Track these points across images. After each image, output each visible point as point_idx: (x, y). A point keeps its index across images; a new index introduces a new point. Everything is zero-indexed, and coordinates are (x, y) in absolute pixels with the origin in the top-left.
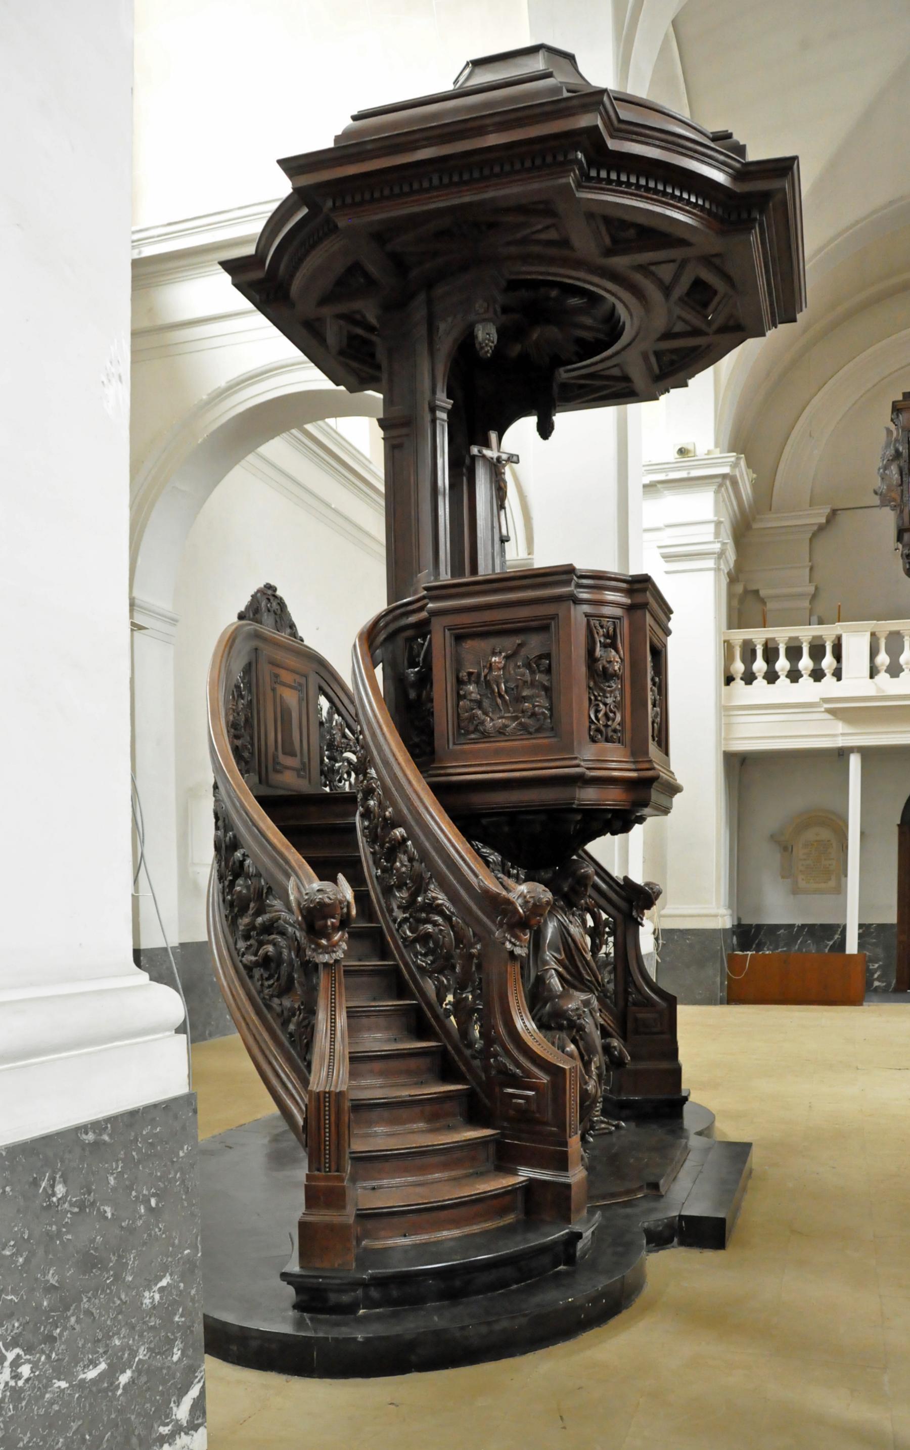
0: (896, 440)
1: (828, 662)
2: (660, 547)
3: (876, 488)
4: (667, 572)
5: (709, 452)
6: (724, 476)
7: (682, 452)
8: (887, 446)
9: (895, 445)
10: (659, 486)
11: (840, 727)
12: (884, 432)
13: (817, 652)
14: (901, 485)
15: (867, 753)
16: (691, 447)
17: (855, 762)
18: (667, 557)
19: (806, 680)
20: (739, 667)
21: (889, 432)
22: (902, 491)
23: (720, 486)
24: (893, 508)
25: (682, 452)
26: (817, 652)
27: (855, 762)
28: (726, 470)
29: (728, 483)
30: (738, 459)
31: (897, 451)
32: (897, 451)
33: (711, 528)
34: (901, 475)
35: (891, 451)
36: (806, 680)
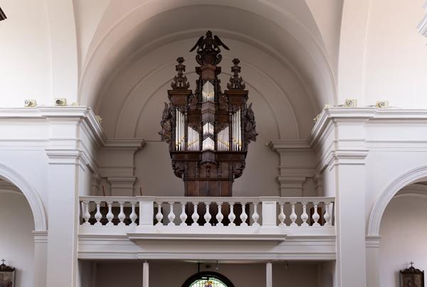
0: (170, 109)
1: (133, 216)
2: (46, 150)
4: (50, 163)
5: (73, 104)
6: (81, 117)
7: (58, 102)
8: (165, 111)
10: (48, 119)
11: (138, 249)
12: (164, 105)
13: (128, 211)
15: (153, 263)
16: (63, 101)
17: (146, 267)
18: (50, 156)
19: (122, 224)
20: (87, 215)
21: (166, 105)
23: (80, 122)
25: (58, 102)
26: (128, 211)
27: (146, 267)
28: (82, 114)
29: (83, 121)
30: (88, 109)
31: (170, 114)
32: (170, 114)
33: (74, 142)
35: (167, 114)
36: (122, 224)
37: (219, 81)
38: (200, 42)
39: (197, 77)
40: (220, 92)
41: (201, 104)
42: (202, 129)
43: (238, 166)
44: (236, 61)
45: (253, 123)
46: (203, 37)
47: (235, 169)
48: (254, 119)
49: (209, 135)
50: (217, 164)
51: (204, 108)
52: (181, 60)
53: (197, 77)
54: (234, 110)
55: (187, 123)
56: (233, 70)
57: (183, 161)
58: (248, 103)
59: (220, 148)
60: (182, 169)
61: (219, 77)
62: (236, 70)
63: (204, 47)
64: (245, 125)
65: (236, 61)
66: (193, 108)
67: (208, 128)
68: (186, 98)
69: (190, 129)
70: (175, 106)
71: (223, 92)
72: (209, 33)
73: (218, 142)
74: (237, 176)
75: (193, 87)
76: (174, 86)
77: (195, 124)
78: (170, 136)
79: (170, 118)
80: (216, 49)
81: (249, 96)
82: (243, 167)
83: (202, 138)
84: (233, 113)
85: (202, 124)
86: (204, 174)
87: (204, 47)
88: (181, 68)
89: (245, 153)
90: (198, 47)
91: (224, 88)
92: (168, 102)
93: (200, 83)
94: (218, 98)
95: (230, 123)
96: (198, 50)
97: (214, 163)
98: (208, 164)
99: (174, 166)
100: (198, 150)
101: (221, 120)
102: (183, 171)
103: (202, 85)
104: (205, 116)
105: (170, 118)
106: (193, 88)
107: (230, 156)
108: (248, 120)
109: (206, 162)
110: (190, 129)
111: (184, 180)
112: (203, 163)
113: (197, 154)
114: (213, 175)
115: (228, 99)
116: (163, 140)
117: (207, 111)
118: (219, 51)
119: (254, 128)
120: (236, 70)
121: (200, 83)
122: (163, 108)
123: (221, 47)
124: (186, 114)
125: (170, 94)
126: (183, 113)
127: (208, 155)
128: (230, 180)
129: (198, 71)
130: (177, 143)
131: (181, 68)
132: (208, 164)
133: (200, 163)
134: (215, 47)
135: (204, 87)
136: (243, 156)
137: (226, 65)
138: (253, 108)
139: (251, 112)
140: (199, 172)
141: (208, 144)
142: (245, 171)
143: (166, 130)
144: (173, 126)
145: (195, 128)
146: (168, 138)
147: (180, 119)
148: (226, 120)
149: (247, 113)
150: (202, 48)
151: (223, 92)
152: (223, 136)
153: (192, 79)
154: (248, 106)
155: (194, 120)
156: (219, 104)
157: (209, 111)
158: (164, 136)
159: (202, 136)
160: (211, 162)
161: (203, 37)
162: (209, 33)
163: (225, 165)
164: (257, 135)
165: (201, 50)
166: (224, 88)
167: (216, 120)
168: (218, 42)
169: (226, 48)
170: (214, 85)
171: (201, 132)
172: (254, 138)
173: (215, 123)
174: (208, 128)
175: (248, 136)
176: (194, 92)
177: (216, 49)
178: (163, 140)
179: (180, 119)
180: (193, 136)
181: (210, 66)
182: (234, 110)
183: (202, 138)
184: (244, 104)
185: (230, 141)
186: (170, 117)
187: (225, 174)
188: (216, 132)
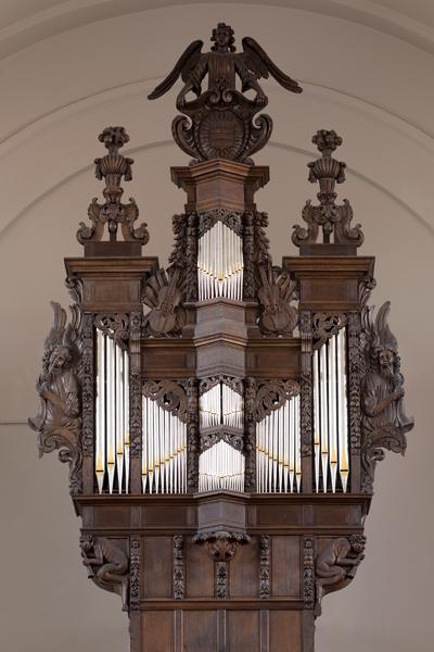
0: (72, 329)
3: (33, 416)
9: (69, 336)
14: (79, 415)
21: (59, 311)
22: (81, 427)
24: (63, 458)
34: (79, 396)
35: (61, 351)
37: (262, 219)
38: (190, 63)
39: (178, 200)
40: (267, 262)
41: (194, 309)
42: (198, 409)
43: (335, 551)
44: (327, 141)
45: (393, 382)
46: (199, 44)
47: (323, 563)
48: (396, 365)
49: (222, 433)
50: (256, 543)
51: (203, 327)
52: (114, 138)
53: (178, 200)
54: (321, 331)
55: (140, 383)
56: (316, 173)
57: (125, 534)
58: (375, 300)
59: (261, 488)
60: (122, 564)
61: (263, 199)
62: (327, 173)
63: (205, 86)
64: (364, 392)
65: (327, 141)
66: (162, 324)
67: (221, 404)
68: (135, 285)
69: (150, 408)
70: (94, 317)
71: (277, 262)
72: (223, 34)
73: (261, 458)
74: (331, 588)
75: (161, 246)
76: (87, 238)
77: (169, 387)
78: (71, 430)
79: (72, 364)
80: (250, 95)
81: (376, 276)
82: (356, 553)
83: (197, 443)
84: (316, 342)
85: (199, 388)
86: (204, 584)
87: (205, 86)
88: (114, 169)
89: (364, 503)
90: (179, 84)
91: (281, 247)
92: (67, 301)
93: (190, 227)
94: (260, 286)
95: (304, 382)
96: (182, 95)
97: (244, 542)
98: (218, 546)
99: (89, 552)
100: (184, 488)
101: (273, 373)
102: (127, 571)
103: (198, 235)
104: (205, 359)
105: (72, 364)
106: (161, 246)
107: (308, 512)
108: (374, 369)
109: (212, 540)
110: (150, 408)
111: (130, 606)
112: (200, 542)
113: (173, 511)
114: (240, 586)
115: (298, 288)
116: (45, 448)
117: (220, 333)
118: (261, 102)
119: (398, 400)
120: (327, 173)
121: (190, 227)
122: (48, 322)
123: (268, 84)
124: (135, 349)
125: (75, 273)
126: (125, 343)
127: (221, 507)
128: (307, 606)
129: (181, 177)
130: (100, 465)
131: (114, 169)
132: (218, 546)
133: (189, 542)
134: (245, 88)
135: (203, 241)
136: (356, 510)
137: (291, 129)
138: (393, 323)
139: (387, 337)
140: (187, 576)
141: (221, 466)
142: (361, 571)
143: (59, 412)
144: (86, 395)
145: (171, 403)
146: (66, 442)
147: (113, 366)
148: (286, 373)
149: (370, 341)
150: (197, 90)
151: (277, 262)
152: (279, 433)
153: (156, 201)
154: (373, 317)
155: (168, 372)
156: (261, 308)
157: (218, 340)
158: (50, 434)
159: (198, 436)
160: (232, 540)
161: (199, 44)
162: (223, 34)
163: (284, 549)
164: (410, 426)
165: (191, 97)
166: (281, 247)
167: (249, 372)
168: (257, 61)
169: (290, 85)
170: (243, 234)
171: (193, 420)
172: (395, 437)
173: (245, 383)
174: (221, 404)
175: (376, 430)
176: (165, 264)
177: (250, 95)
178: (45, 448)
179: (113, 366)
180: (164, 436)
181: (227, 166)
182: (321, 331)
183: (197, 443)
184: (359, 308)
185: (304, 454)
186: (73, 358)
187: (287, 581)
188: (250, 419)
